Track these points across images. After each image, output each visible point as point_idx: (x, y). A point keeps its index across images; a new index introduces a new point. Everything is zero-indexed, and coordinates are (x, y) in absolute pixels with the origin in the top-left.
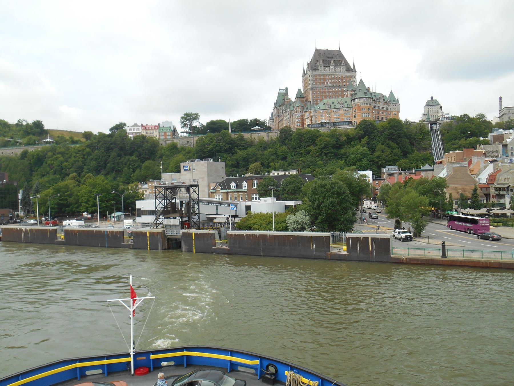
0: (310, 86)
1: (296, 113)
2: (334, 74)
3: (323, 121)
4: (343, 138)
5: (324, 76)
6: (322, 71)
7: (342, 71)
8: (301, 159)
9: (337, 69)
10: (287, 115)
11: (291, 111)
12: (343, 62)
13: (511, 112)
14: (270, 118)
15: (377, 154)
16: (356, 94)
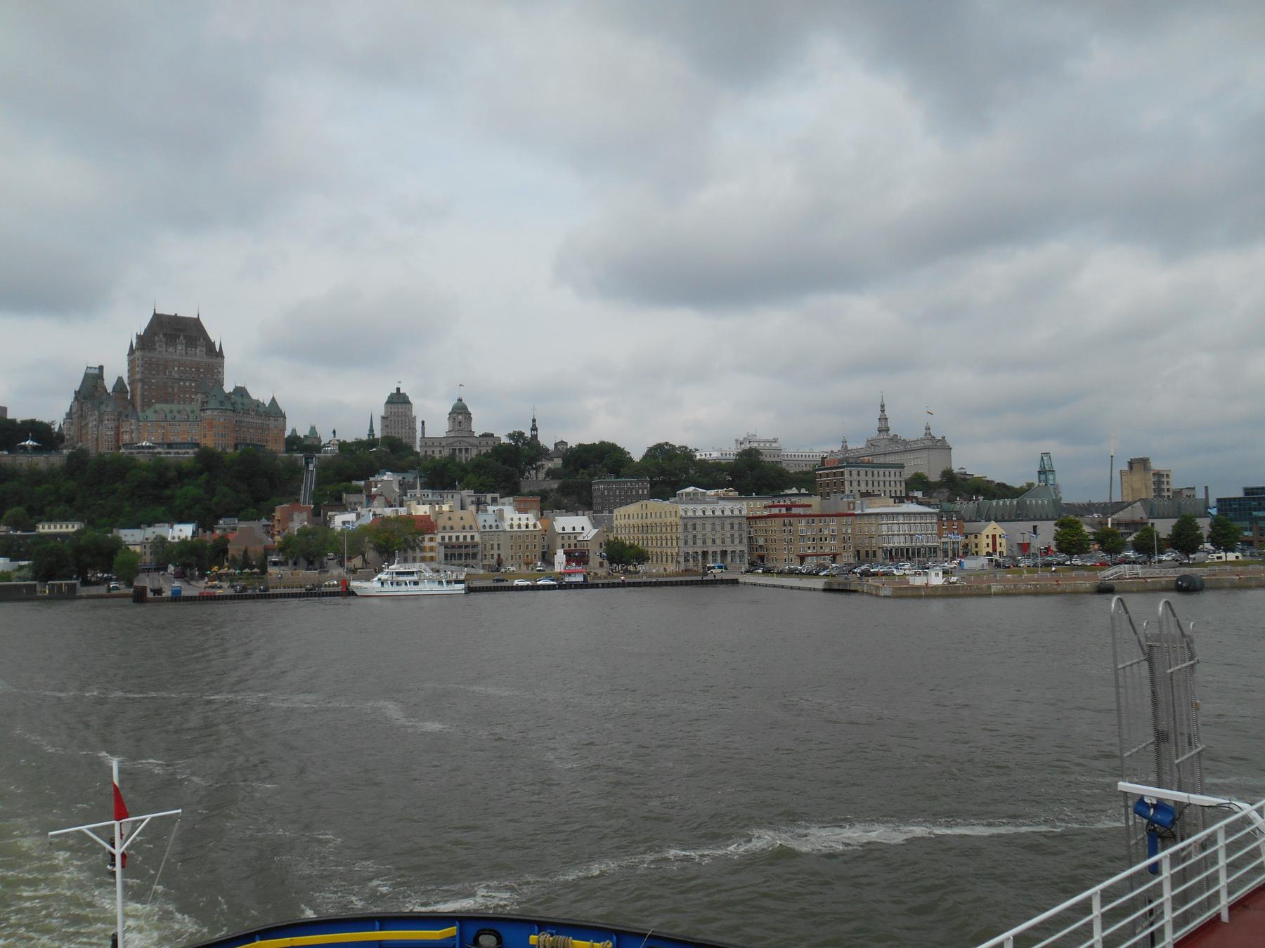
0: (138, 376)
1: (106, 422)
2: (184, 358)
3: (144, 444)
4: (172, 474)
5: (166, 361)
6: (163, 352)
7: (199, 354)
8: (99, 502)
9: (191, 351)
10: (92, 421)
11: (101, 415)
12: (202, 340)
13: (428, 444)
14: (67, 414)
15: (215, 499)
16: (207, 402)
